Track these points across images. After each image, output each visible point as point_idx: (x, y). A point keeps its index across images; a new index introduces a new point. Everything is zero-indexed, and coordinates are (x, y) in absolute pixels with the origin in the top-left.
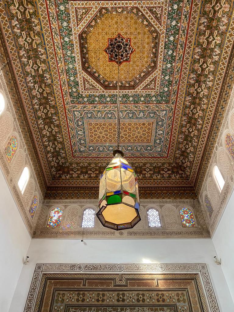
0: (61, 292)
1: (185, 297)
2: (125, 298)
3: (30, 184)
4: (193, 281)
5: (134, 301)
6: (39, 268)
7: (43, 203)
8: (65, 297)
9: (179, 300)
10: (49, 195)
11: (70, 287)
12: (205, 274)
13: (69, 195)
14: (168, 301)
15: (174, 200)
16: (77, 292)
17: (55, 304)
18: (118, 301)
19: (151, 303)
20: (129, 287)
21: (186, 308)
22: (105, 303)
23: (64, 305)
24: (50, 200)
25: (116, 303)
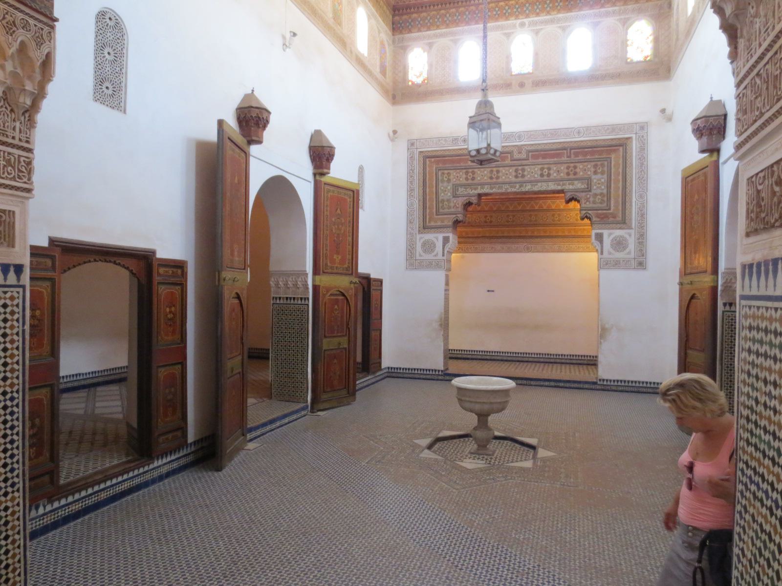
0: (446, 172)
1: (606, 169)
2: (526, 173)
3: (371, 29)
4: (621, 148)
5: (536, 176)
6: (413, 144)
7: (394, 42)
8: (452, 177)
9: (595, 173)
10: (399, 25)
11: (455, 165)
12: (643, 137)
13: (431, 21)
14: (581, 173)
15: (622, 8)
16: (464, 171)
17: (440, 184)
18: (516, 177)
19: (558, 177)
20: (531, 161)
21: (603, 180)
22: (500, 180)
23: (451, 184)
24: (402, 36)
25: (514, 179)
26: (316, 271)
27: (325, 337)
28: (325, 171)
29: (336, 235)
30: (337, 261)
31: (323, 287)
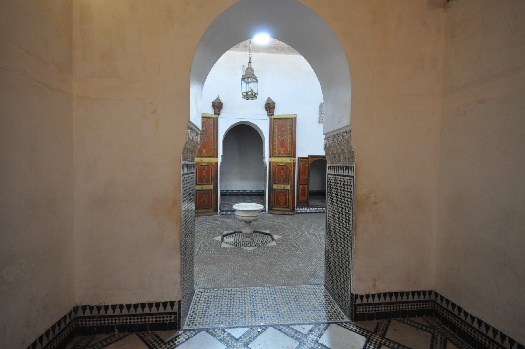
26: (270, 156)
27: (275, 183)
28: (273, 114)
29: (281, 140)
30: (282, 151)
31: (273, 162)
